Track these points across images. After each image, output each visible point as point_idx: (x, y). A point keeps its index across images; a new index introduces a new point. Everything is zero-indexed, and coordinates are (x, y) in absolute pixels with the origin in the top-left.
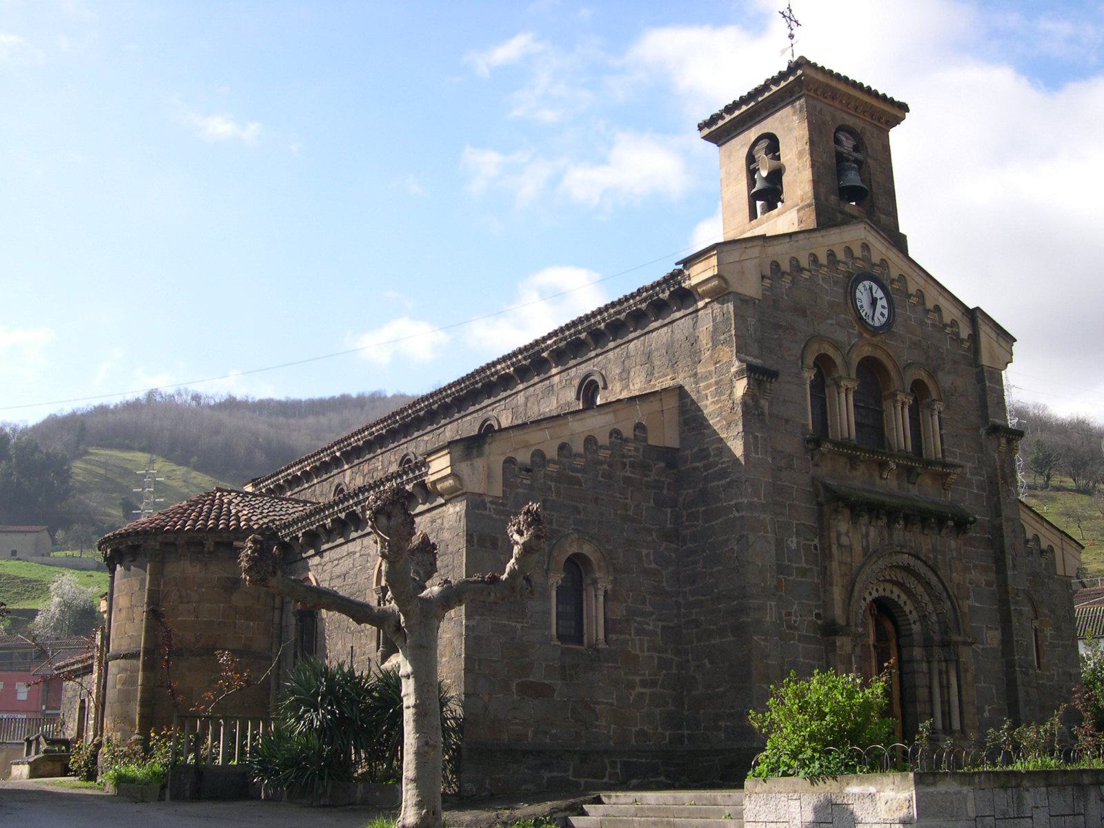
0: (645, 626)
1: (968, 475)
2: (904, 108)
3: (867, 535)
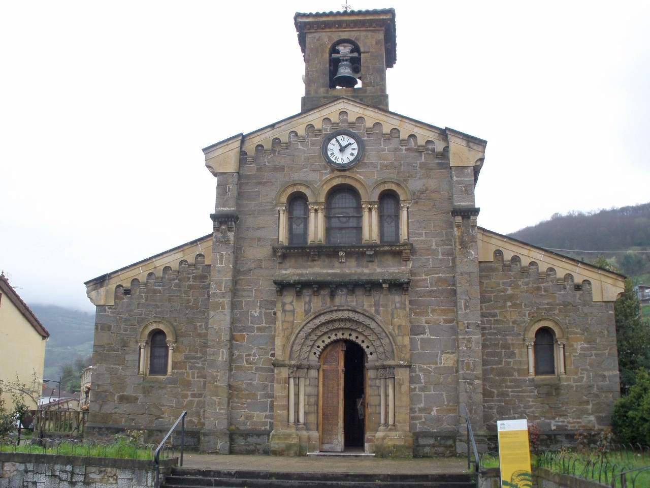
0: (197, 365)
1: (434, 247)
2: (391, 12)
3: (310, 302)
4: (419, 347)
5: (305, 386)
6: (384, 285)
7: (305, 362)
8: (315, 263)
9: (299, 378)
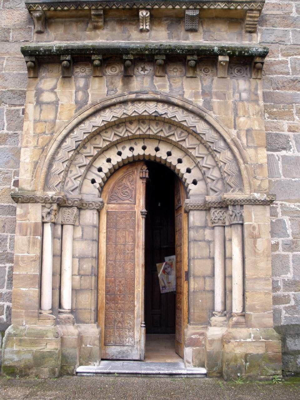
3: (86, 87)
4: (281, 172)
5: (74, 239)
6: (220, 58)
7: (75, 195)
8: (98, 32)
9: (62, 226)
